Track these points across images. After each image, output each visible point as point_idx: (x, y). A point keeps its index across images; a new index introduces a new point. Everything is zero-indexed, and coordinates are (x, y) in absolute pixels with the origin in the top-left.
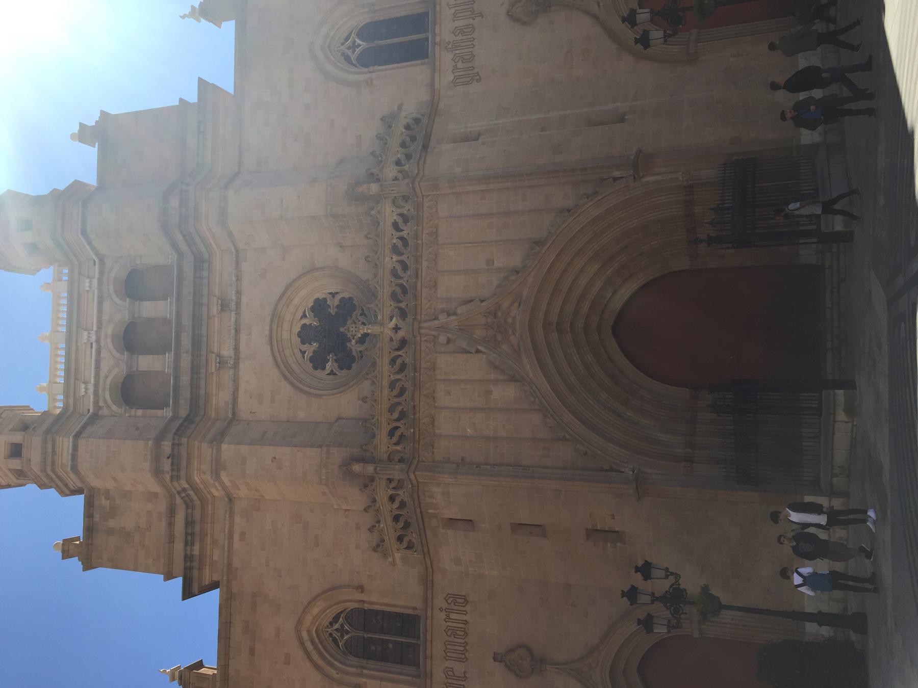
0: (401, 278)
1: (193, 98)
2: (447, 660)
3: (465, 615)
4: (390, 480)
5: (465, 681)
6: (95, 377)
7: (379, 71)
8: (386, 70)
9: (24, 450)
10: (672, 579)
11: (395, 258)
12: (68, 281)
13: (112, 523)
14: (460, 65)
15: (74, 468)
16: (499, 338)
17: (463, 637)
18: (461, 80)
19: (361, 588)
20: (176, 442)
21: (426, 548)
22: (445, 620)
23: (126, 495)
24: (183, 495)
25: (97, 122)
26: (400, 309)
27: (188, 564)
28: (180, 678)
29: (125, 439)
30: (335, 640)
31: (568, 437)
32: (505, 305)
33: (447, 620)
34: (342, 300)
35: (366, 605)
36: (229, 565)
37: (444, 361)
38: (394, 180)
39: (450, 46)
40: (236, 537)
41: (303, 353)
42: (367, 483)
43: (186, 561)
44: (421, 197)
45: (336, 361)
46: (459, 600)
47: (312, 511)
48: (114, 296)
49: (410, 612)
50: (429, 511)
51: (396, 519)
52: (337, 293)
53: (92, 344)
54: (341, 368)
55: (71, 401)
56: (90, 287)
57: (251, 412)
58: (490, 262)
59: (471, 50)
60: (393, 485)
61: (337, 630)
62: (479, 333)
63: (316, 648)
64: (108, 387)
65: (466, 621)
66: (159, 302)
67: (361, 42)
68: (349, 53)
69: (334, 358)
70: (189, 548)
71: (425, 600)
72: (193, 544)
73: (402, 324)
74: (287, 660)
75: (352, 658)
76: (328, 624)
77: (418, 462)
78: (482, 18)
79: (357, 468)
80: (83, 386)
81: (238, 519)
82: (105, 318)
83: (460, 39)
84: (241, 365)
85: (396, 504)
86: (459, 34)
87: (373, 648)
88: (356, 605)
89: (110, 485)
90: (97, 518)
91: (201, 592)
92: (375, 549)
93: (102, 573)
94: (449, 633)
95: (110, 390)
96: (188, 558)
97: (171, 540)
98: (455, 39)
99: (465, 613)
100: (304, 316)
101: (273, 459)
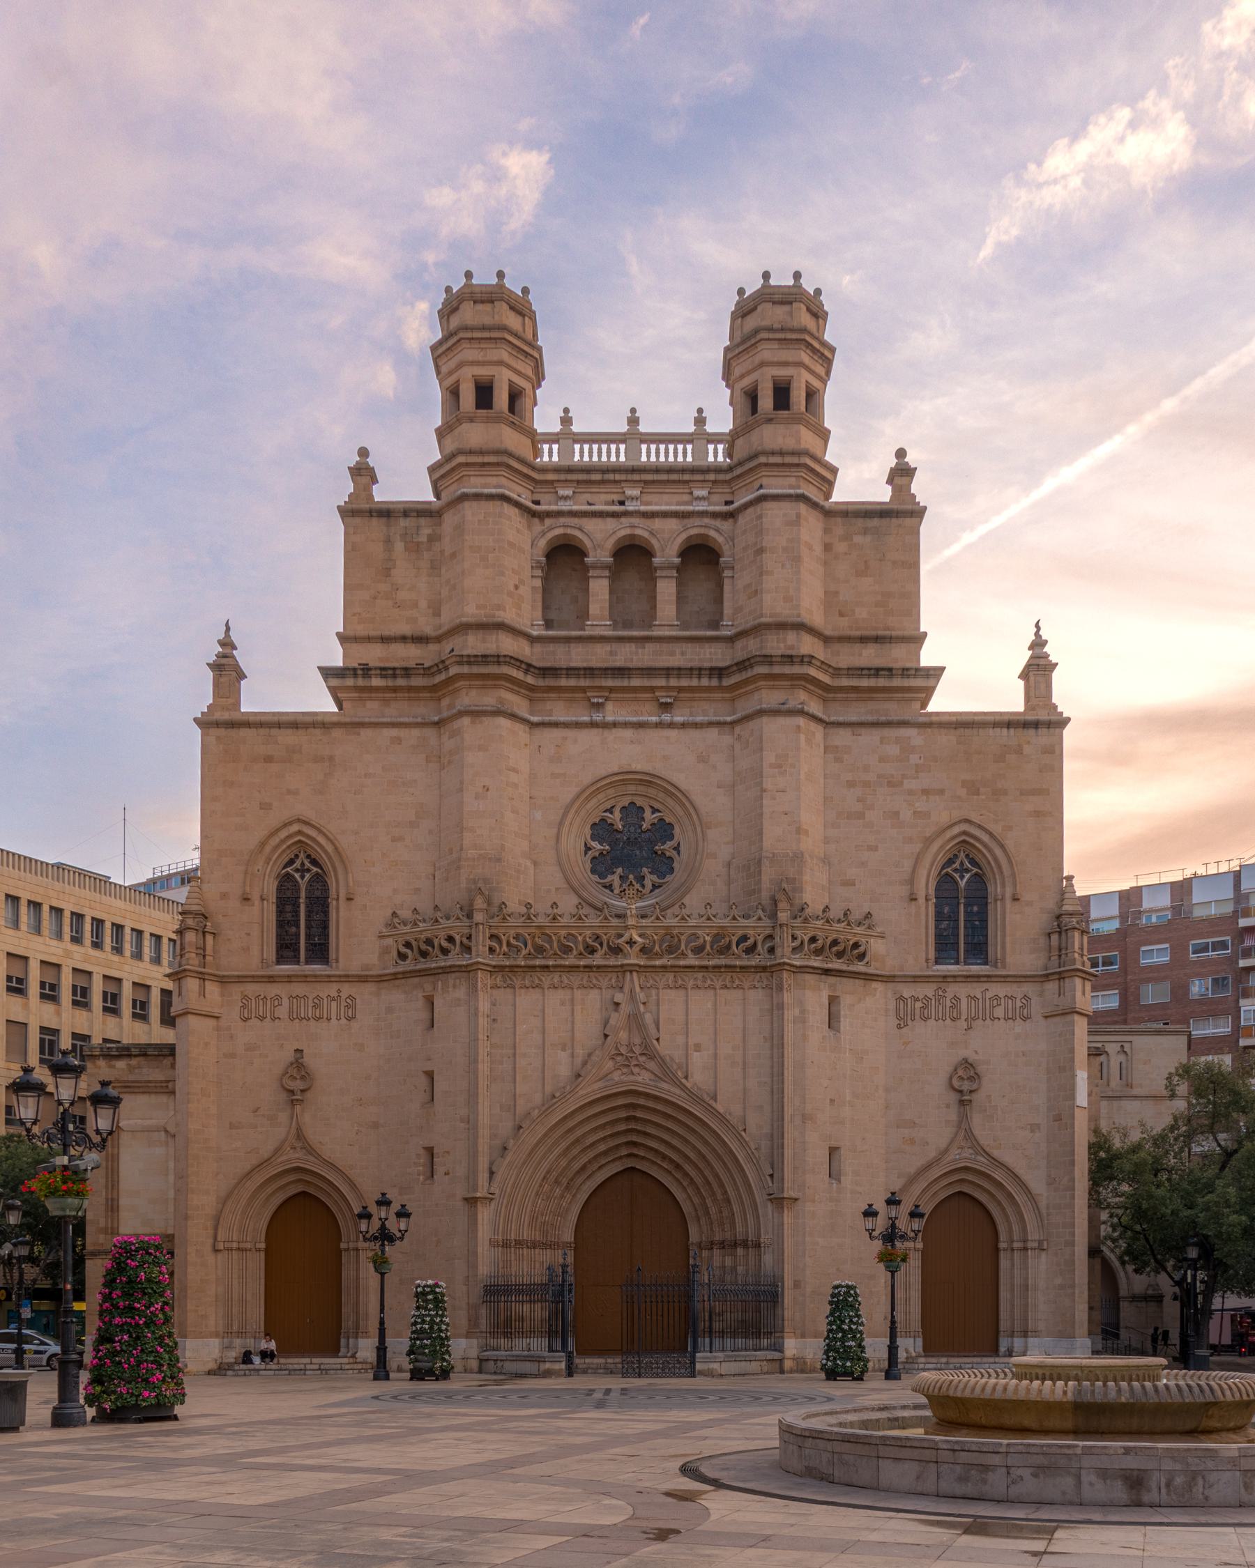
8: (927, 915)
14: (919, 1005)
16: (619, 1058)
18: (902, 1006)
20: (502, 659)
21: (401, 976)
23: (435, 567)
25: (914, 496)
27: (360, 672)
28: (225, 656)
31: (521, 1130)
35: (334, 902)
36: (362, 725)
39: (940, 993)
40: (394, 732)
46: (350, 1011)
47: (430, 832)
48: (684, 536)
51: (429, 942)
53: (622, 503)
55: (550, 477)
56: (698, 498)
60: (465, 941)
63: (283, 841)
64: (569, 531)
66: (674, 607)
68: (954, 866)
70: (378, 672)
73: (636, 948)
74: (265, 806)
75: (276, 883)
81: (416, 732)
82: (657, 524)
84: (595, 731)
85: (445, 944)
90: (403, 522)
91: (329, 687)
92: (394, 914)
94: (316, 1001)
97: (385, 640)
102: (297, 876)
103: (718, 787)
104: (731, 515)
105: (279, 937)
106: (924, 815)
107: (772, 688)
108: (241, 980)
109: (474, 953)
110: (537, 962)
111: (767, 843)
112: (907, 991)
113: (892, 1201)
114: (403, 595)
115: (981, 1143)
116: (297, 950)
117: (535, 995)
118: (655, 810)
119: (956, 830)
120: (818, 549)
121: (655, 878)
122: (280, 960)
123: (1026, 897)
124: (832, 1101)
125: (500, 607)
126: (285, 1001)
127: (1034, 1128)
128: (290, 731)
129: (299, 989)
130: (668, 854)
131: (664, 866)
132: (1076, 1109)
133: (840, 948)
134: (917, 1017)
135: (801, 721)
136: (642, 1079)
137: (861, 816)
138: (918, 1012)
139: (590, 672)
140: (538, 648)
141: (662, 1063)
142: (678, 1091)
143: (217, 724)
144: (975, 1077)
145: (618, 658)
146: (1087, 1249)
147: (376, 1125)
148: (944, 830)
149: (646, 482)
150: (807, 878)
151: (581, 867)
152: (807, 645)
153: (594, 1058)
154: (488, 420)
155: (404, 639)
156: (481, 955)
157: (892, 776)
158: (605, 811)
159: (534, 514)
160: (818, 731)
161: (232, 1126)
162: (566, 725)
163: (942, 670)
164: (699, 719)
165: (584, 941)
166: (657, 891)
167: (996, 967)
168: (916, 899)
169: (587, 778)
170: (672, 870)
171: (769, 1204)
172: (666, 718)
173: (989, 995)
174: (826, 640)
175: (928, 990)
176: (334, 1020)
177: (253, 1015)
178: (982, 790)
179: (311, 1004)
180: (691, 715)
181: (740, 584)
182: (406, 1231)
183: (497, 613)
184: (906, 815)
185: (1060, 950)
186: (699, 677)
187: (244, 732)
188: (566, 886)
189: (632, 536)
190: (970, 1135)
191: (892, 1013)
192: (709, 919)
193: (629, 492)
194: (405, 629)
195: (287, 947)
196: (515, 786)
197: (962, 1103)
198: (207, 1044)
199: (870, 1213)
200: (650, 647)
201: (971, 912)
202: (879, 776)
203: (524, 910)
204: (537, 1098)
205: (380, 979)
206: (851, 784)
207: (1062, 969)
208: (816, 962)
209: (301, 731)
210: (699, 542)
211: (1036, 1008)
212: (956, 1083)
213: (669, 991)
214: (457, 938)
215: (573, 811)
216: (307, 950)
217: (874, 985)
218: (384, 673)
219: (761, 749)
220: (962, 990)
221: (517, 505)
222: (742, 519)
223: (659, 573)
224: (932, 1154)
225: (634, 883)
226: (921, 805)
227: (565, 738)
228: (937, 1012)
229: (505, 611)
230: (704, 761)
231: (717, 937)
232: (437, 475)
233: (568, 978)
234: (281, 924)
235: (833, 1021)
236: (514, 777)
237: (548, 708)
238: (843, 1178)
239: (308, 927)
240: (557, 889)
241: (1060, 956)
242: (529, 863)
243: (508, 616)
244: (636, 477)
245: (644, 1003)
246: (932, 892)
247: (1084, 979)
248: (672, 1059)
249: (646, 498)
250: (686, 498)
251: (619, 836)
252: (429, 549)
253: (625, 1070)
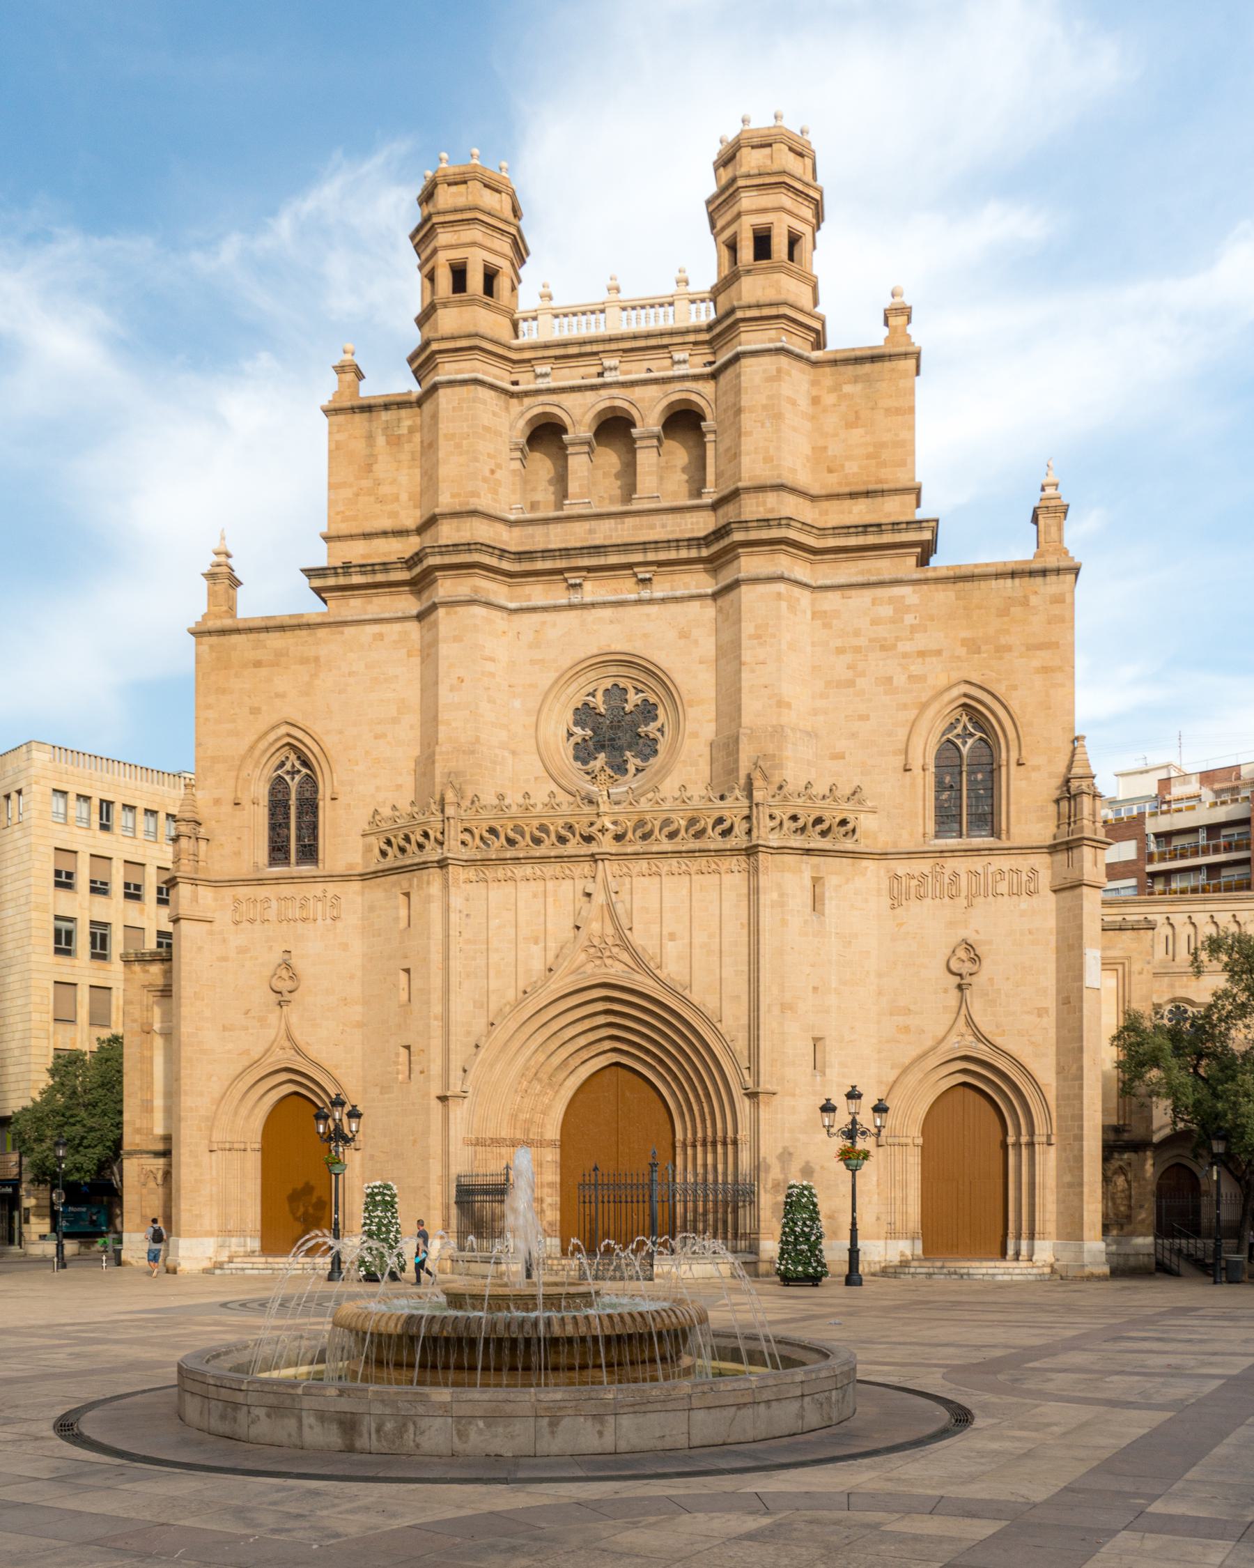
14: (914, 883)
16: (592, 950)
18: (895, 885)
39: (938, 869)
48: (665, 403)
50: (415, 879)
53: (600, 375)
55: (527, 355)
56: (679, 362)
59: (930, 895)
60: (439, 836)
63: (271, 744)
64: (548, 409)
67: (968, 746)
68: (956, 732)
73: (609, 836)
81: (397, 627)
82: (638, 392)
84: (573, 613)
90: (385, 416)
94: (303, 902)
95: (544, 414)
97: (367, 536)
102: (287, 778)
103: (701, 663)
104: (714, 376)
105: (271, 840)
106: (921, 679)
107: (751, 554)
108: (232, 883)
109: (445, 847)
110: (509, 855)
111: (746, 719)
112: (902, 868)
113: (853, 1095)
114: (385, 490)
115: (982, 1030)
116: (288, 852)
117: (509, 888)
118: (638, 691)
119: (956, 692)
120: (804, 403)
121: (638, 761)
122: (273, 861)
123: (1031, 760)
124: (815, 989)
125: (475, 494)
126: (274, 904)
127: (1041, 1012)
128: (277, 634)
129: (286, 890)
130: (651, 736)
131: (648, 748)
132: (1085, 989)
133: (824, 826)
134: (913, 896)
135: (781, 587)
136: (616, 971)
137: (851, 683)
138: (913, 891)
139: (566, 552)
140: (517, 531)
141: (635, 955)
142: (651, 982)
143: (210, 633)
144: (976, 959)
145: (597, 536)
146: (1100, 1144)
147: (360, 1025)
148: (941, 693)
149: (625, 351)
150: (788, 753)
151: (565, 751)
152: (789, 506)
153: (565, 951)
154: (462, 303)
155: (385, 534)
156: (453, 849)
157: (885, 639)
158: (588, 695)
159: (512, 395)
160: (805, 596)
161: (225, 1028)
162: (545, 609)
164: (678, 593)
165: (557, 832)
166: (640, 775)
167: (999, 838)
168: (910, 770)
169: (566, 662)
170: (656, 752)
171: (746, 1100)
172: (645, 594)
173: (991, 869)
174: (813, 498)
175: (924, 866)
176: (319, 921)
178: (984, 648)
179: (298, 905)
180: (672, 590)
181: (721, 449)
182: (357, 1132)
183: (472, 500)
184: (900, 680)
185: (1069, 818)
186: (678, 548)
187: (235, 638)
188: (546, 775)
189: (613, 408)
190: (970, 1022)
191: (885, 893)
192: (684, 802)
193: (608, 362)
194: (387, 524)
195: (279, 850)
196: (492, 675)
197: (960, 987)
198: (200, 949)
199: (828, 1108)
200: (630, 522)
201: (976, 780)
202: (871, 640)
203: (496, 802)
204: (511, 995)
205: (364, 877)
206: (840, 651)
207: (1071, 838)
208: (797, 841)
209: (289, 634)
210: (683, 407)
211: (1045, 879)
212: (955, 966)
213: (642, 878)
214: (431, 833)
215: (552, 696)
216: (298, 851)
217: (865, 863)
218: (363, 569)
219: (739, 621)
220: (961, 865)
221: (492, 387)
223: (639, 444)
224: (929, 1043)
225: (606, 768)
226: (916, 668)
227: (544, 623)
228: (934, 890)
229: (479, 496)
230: (686, 638)
231: (692, 821)
232: (416, 365)
233: (541, 870)
234: (274, 827)
235: (817, 902)
236: (489, 667)
237: (527, 592)
238: (827, 1071)
239: (299, 828)
240: (536, 778)
241: (1069, 824)
242: (506, 754)
243: (484, 502)
244: (614, 346)
245: (617, 893)
247: (1096, 847)
248: (644, 949)
249: (625, 367)
251: (601, 720)
252: (410, 441)
253: (598, 962)
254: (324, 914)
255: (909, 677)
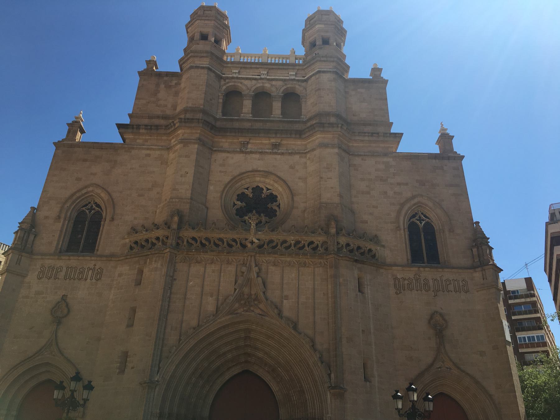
0: (281, 245)
1: (393, 130)
2: (67, 268)
3: (90, 279)
4: (167, 238)
5: (54, 278)
6: (242, 77)
7: (405, 235)
8: (405, 239)
9: (203, 41)
10: (82, 402)
11: (293, 242)
12: (299, 63)
13: (162, 86)
14: (406, 282)
15: (191, 67)
17: (78, 278)
18: (397, 282)
19: (113, 219)
20: (200, 121)
22: (89, 267)
23: (176, 94)
24: (172, 125)
26: (263, 245)
27: (135, 127)
28: (76, 122)
29: (205, 94)
30: (87, 205)
32: (261, 306)
33: (89, 268)
34: (276, 211)
37: (231, 269)
38: (337, 242)
39: (417, 277)
40: (148, 152)
41: (247, 189)
42: (167, 225)
43: (137, 125)
44: (327, 258)
45: (241, 207)
47: (158, 193)
48: (285, 87)
49: (96, 248)
50: (148, 260)
52: (279, 208)
53: (260, 76)
54: (237, 210)
55: (229, 65)
57: (215, 160)
58: (287, 298)
59: (415, 289)
61: (92, 206)
62: (246, 290)
63: (83, 195)
65: (87, 279)
67: (423, 224)
68: (417, 217)
69: (243, 206)
70: (144, 127)
71: (101, 256)
72: (145, 129)
73: (255, 245)
74: (78, 179)
75: (76, 214)
76: (96, 202)
77: (176, 254)
78: (434, 296)
79: (176, 219)
80: (237, 71)
81: (158, 152)
82: (274, 83)
83: (422, 283)
84: (242, 155)
85: (154, 241)
86: (425, 282)
87: (80, 226)
88: (104, 217)
89: (183, 85)
90: (165, 78)
91: (120, 133)
93: (136, 80)
96: (138, 127)
97: (150, 117)
98: (421, 280)
99: (91, 279)
100: (268, 189)
101: (187, 173)
119: (416, 200)
137: (368, 193)
138: (406, 286)
163: (402, 134)
176: (88, 280)
177: (45, 276)
179: (78, 271)
204: (194, 323)
215: (228, 186)
222: (310, 82)
227: (227, 157)
244: (266, 66)
246: (406, 226)
250: (287, 75)
254: (92, 277)
255: (394, 192)
